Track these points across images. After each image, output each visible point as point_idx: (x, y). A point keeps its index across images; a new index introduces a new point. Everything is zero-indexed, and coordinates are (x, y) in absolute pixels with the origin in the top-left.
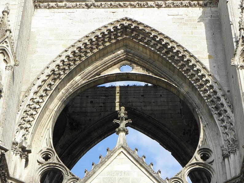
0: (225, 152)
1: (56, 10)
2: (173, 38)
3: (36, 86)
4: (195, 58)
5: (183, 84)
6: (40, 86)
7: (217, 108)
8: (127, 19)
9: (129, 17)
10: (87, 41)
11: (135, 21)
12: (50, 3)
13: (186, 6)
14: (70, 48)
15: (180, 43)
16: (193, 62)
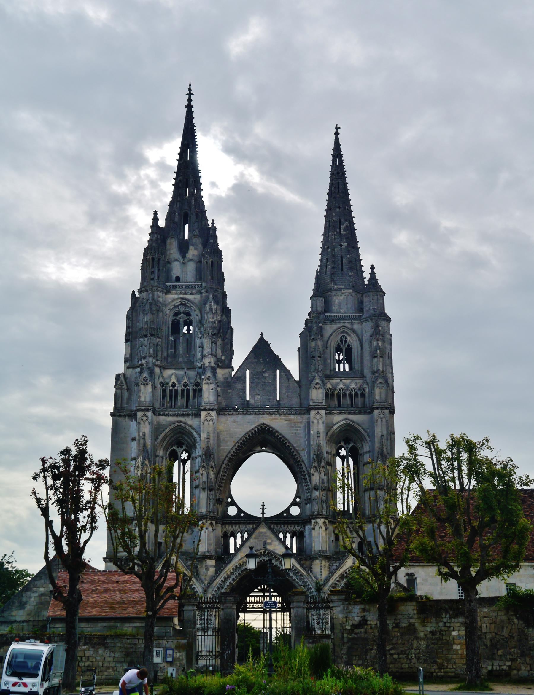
0: (306, 502)
1: (228, 416)
2: (287, 437)
3: (223, 468)
4: (297, 451)
5: (291, 459)
6: (224, 468)
7: (304, 479)
8: (264, 424)
9: (265, 422)
10: (244, 439)
11: (268, 426)
12: (225, 413)
13: (293, 414)
14: (236, 444)
15: (290, 440)
16: (295, 453)
